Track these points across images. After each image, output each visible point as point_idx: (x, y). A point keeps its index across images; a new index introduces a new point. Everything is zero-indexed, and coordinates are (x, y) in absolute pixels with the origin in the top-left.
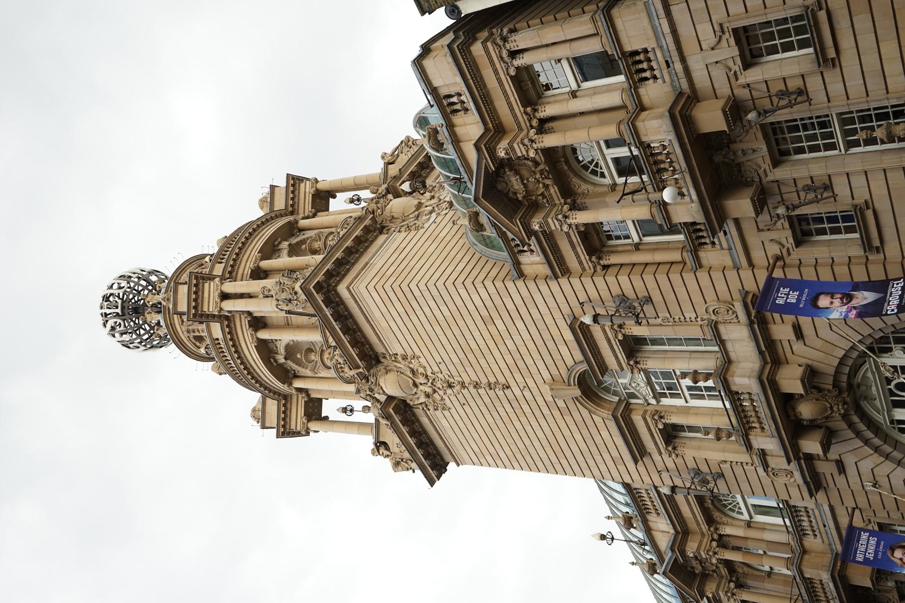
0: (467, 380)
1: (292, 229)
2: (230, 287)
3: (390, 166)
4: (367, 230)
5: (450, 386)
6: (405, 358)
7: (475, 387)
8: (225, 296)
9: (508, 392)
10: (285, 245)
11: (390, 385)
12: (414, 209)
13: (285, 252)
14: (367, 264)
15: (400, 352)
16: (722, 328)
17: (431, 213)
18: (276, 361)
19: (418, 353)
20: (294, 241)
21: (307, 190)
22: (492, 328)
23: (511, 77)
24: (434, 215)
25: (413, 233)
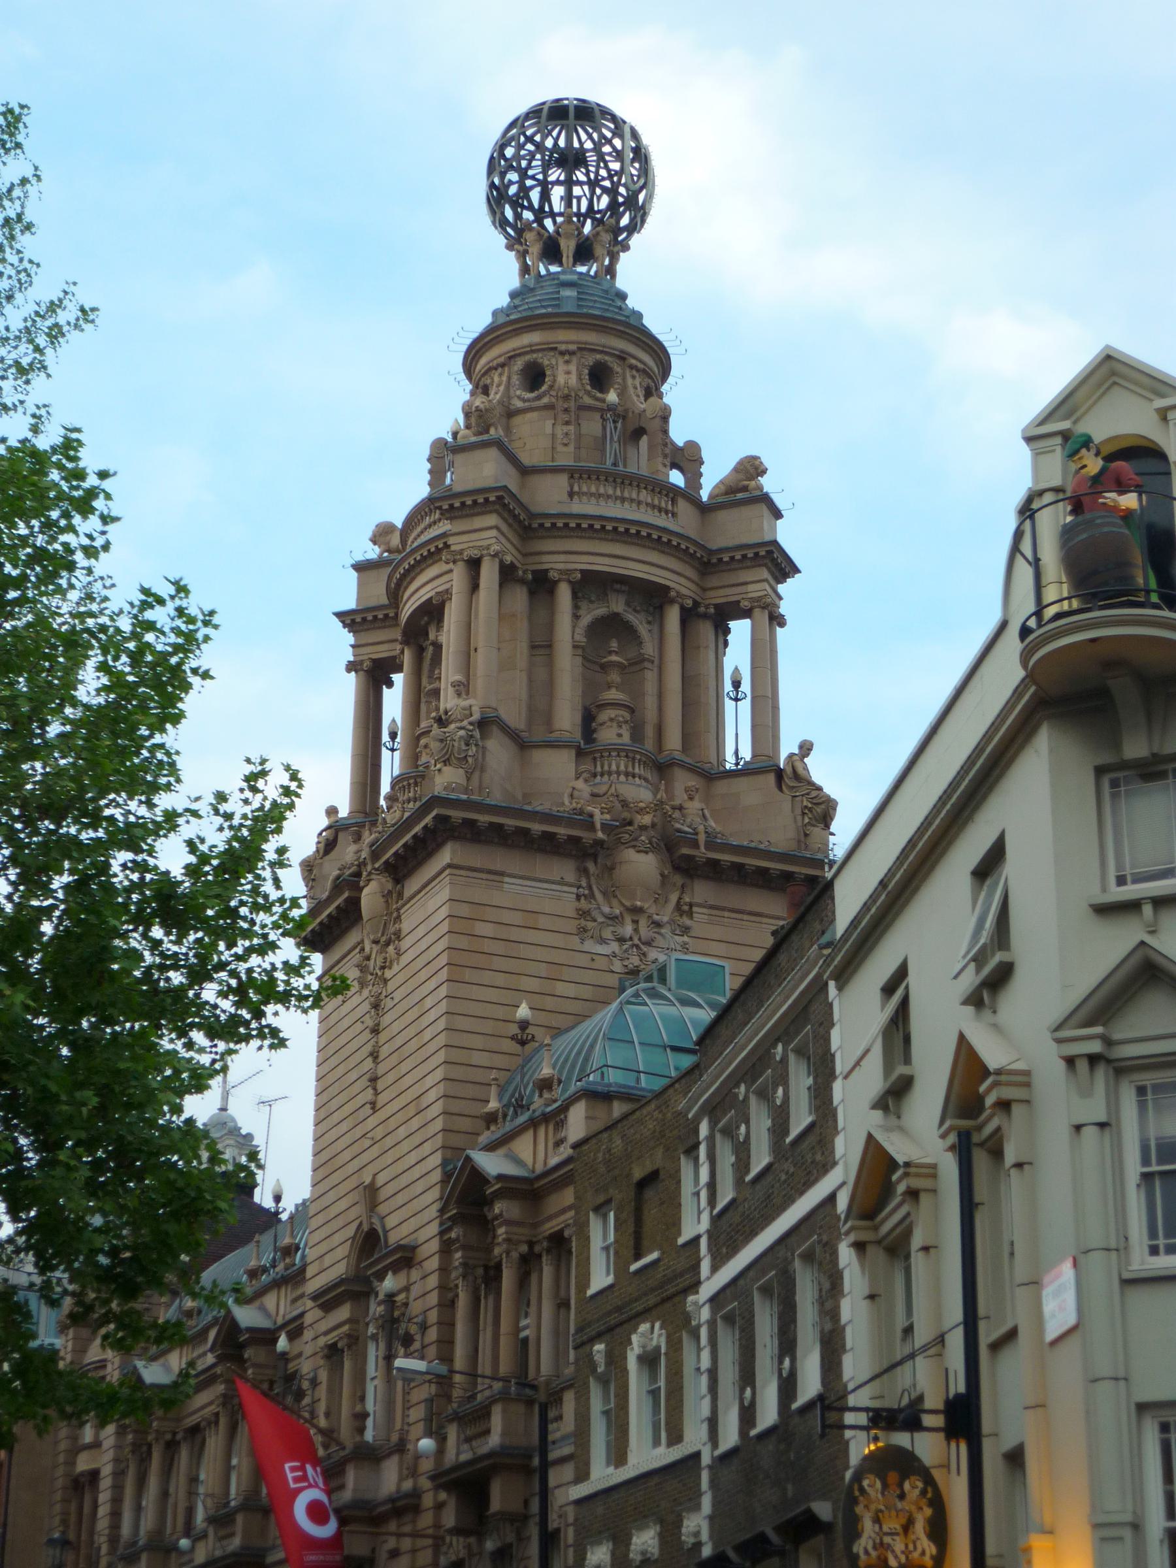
0: (383, 1037)
1: (653, 597)
2: (489, 574)
3: (771, 778)
4: (576, 840)
5: (376, 1006)
6: (398, 936)
7: (371, 1054)
8: (474, 565)
9: (367, 1110)
10: (617, 605)
11: (370, 896)
12: (628, 904)
13: (601, 611)
14: (502, 874)
15: (406, 926)
16: (395, 1459)
17: (621, 940)
18: (428, 624)
19: (405, 959)
20: (631, 617)
21: (751, 587)
22: (412, 1110)
23: (562, 1230)
24: (614, 947)
25: (571, 926)
